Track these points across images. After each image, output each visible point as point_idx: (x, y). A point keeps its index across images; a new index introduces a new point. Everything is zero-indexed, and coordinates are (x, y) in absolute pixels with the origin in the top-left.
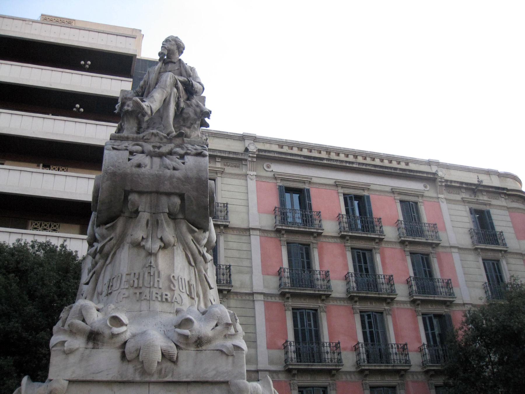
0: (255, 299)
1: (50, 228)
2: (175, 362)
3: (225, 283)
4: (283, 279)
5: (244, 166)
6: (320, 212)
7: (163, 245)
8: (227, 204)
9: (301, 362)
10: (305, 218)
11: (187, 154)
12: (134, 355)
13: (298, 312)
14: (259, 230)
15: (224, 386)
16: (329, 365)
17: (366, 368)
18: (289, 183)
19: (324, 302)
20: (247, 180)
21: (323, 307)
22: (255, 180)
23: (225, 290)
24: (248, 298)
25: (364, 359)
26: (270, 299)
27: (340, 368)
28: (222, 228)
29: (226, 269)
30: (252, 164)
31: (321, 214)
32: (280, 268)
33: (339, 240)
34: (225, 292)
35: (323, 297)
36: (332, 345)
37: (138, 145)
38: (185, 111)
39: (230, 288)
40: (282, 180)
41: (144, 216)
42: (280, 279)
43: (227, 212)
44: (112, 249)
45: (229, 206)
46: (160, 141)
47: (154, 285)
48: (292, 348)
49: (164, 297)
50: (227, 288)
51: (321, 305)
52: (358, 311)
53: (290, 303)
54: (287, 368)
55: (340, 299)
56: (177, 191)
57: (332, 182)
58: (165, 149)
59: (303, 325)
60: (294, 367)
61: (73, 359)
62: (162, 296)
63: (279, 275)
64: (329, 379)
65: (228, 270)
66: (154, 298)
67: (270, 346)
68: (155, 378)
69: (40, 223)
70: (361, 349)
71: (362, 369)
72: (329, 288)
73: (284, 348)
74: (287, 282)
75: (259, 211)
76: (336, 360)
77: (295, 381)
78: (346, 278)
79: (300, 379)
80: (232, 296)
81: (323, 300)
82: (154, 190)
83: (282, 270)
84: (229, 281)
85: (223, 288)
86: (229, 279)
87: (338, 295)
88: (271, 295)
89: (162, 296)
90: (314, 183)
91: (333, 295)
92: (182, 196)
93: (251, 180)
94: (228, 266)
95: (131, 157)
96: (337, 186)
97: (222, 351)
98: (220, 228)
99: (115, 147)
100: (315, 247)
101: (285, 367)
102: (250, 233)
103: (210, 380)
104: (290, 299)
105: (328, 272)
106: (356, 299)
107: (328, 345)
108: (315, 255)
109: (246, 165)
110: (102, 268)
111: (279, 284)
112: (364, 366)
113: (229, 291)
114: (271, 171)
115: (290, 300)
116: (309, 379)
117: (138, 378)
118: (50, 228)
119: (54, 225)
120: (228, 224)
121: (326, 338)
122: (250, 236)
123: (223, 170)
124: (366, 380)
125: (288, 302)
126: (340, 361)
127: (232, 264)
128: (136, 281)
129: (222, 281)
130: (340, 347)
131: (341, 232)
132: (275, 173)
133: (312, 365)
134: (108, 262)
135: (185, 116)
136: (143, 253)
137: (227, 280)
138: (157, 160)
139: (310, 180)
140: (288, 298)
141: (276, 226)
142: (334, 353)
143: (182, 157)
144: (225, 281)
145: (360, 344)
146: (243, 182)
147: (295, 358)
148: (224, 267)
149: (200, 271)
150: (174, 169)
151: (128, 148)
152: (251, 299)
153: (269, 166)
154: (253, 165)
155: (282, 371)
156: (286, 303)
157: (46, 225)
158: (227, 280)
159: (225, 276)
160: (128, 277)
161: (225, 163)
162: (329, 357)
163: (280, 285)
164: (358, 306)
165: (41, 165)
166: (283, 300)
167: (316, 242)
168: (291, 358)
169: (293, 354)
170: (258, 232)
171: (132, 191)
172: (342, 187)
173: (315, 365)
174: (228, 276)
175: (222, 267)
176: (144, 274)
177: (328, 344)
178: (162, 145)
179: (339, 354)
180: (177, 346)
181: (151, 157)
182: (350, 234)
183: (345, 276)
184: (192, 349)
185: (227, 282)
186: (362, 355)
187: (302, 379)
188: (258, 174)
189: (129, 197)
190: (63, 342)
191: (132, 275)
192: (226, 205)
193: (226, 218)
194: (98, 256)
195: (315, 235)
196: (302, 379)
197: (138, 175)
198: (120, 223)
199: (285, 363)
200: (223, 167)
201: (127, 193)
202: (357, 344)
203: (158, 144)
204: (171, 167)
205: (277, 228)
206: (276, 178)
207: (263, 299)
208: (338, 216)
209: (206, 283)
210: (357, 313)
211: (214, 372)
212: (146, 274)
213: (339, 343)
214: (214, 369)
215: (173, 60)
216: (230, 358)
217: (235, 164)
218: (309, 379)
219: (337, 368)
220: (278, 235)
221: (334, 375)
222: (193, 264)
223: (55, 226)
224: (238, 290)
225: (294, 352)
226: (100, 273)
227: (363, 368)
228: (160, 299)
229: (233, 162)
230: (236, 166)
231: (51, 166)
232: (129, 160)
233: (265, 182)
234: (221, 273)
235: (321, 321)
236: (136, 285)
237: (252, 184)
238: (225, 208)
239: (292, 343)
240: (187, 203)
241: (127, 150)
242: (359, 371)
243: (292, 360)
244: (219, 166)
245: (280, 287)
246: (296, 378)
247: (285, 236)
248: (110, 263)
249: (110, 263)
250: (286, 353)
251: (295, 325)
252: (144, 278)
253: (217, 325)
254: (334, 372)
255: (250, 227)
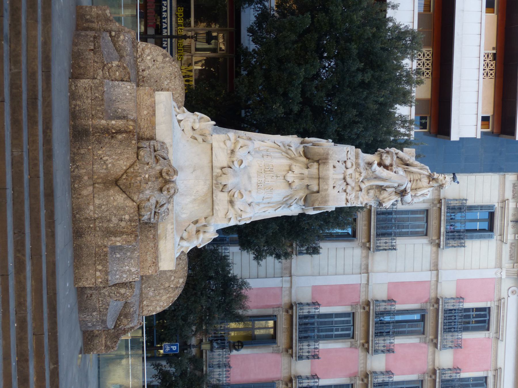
0: (362, 275)
1: (426, 69)
2: (222, 191)
3: (377, 244)
4: (384, 304)
5: (512, 265)
6: (461, 347)
7: (290, 182)
8: (464, 246)
9: (299, 318)
10: (453, 330)
11: (347, 193)
12: (225, 173)
13: (351, 319)
14: (437, 281)
15: (212, 213)
16: (296, 346)
17: (294, 384)
18: (495, 315)
19: (361, 346)
20: (495, 268)
21: (356, 345)
22: (494, 276)
23: (370, 245)
24: (363, 267)
25: (302, 383)
26: (363, 289)
27: (294, 357)
28: (437, 241)
29: (392, 246)
30: (514, 273)
31: (460, 349)
32: (395, 302)
33: (431, 367)
34: (368, 245)
35: (366, 346)
36: (316, 350)
37: (352, 165)
38: (385, 192)
39: (371, 249)
40: (498, 307)
41: (306, 172)
42: (383, 301)
43: (455, 247)
44: (290, 155)
45: (463, 248)
46: (357, 178)
47: (267, 179)
48: (313, 311)
49: (260, 185)
50: (372, 246)
51: (358, 342)
52: (353, 382)
53: (359, 310)
54: (293, 304)
55: (365, 363)
56: (320, 189)
57: (500, 364)
58: (349, 180)
59: (336, 322)
60: (294, 311)
61: (222, 145)
62: (260, 183)
63: (389, 300)
64: (284, 347)
65: (390, 248)
66: (259, 179)
67: (316, 289)
68: (214, 182)
69: (429, 59)
70: (313, 381)
71: (292, 380)
72: (376, 351)
73: (313, 303)
74: (381, 307)
75: (458, 281)
76: (302, 354)
77: (281, 312)
78: (388, 372)
79: (283, 318)
80: (364, 251)
81: (363, 345)
82: (320, 176)
83: (393, 303)
84: (379, 248)
85: (372, 243)
86: (381, 248)
87: (369, 362)
88: (367, 292)
89: (260, 183)
90: (497, 344)
91: (369, 356)
92: (318, 192)
93: (496, 273)
94: (395, 248)
95: (340, 162)
96: (496, 370)
97: (228, 212)
98: (438, 239)
99: (349, 153)
100: (421, 340)
101: (295, 303)
102: (433, 270)
103: (214, 207)
104: (363, 310)
105: (393, 352)
106: (365, 380)
107: (316, 346)
108: (413, 340)
109: (514, 268)
110: (281, 150)
111: (378, 299)
112: (295, 383)
113: (369, 248)
114: (508, 295)
115: (362, 310)
116: (283, 326)
117: (214, 174)
118: (426, 69)
119: (429, 72)
120: (441, 247)
121: (323, 346)
122: (430, 271)
123: (504, 242)
124: (282, 384)
125: (361, 309)
126: (300, 358)
127: (398, 251)
128: (268, 170)
129: (379, 242)
130: (315, 359)
131: (439, 369)
132: (506, 299)
133: (296, 329)
134: (283, 153)
135: (382, 192)
136: (284, 173)
137: (380, 246)
138: (342, 176)
139: (500, 339)
140: (364, 308)
141: (442, 298)
142: (309, 352)
143: (345, 191)
144: (379, 245)
145: (317, 380)
146: (493, 263)
147: (303, 312)
148: (394, 244)
149: (282, 204)
150: (334, 187)
151: (349, 160)
152: (362, 271)
153: (514, 292)
154: (513, 275)
155: (291, 300)
156: (359, 306)
157: (428, 64)
158: (380, 246)
159: (385, 245)
160: (271, 166)
161: (514, 245)
162: (304, 347)
163: (377, 301)
164: (358, 382)
165: (494, 52)
166: (362, 304)
167: (427, 341)
168: (303, 309)
169: (307, 310)
170: (434, 279)
171: (319, 165)
172: (495, 376)
173: (296, 332)
174: (385, 248)
175: (393, 241)
176: (273, 174)
177: (317, 346)
178: (353, 179)
179: (308, 358)
180: (230, 191)
181: (343, 173)
182: (437, 380)
183: (390, 371)
184: (229, 199)
185: (378, 246)
186: (307, 381)
187: (283, 320)
188: (503, 280)
189: (315, 163)
190: (230, 139)
191: (272, 168)
192: (463, 245)
193: (448, 245)
194: (288, 147)
195: (435, 341)
196: (283, 320)
197: (328, 167)
198: (304, 159)
199: (299, 304)
200: (509, 242)
201: (318, 161)
202: (318, 377)
203: (353, 177)
204: (335, 185)
205: (439, 299)
206: (500, 300)
207: (363, 282)
208: (458, 368)
209: (277, 208)
210: (351, 380)
211: (217, 209)
212: (272, 175)
213: (318, 358)
214: (219, 209)
215: (431, 182)
216: (224, 216)
217: (513, 255)
218: (283, 326)
219: (294, 355)
220: (433, 300)
221: (287, 351)
222: (284, 200)
223: (428, 74)
224: (370, 258)
225: (309, 312)
226: (279, 149)
227: (294, 381)
228: (259, 182)
229: (516, 252)
230: (511, 256)
231: (494, 62)
232: (339, 161)
233: (494, 289)
234: (387, 241)
235: (342, 342)
236: (266, 170)
237: (491, 274)
238: (459, 245)
239: (318, 310)
240: (314, 194)
241: (347, 159)
242: (291, 378)
243: (301, 309)
244: (509, 238)
245: (375, 300)
246: (284, 313)
247: (432, 308)
248: (282, 155)
249: (282, 155)
250: (308, 304)
251: (338, 315)
252: (269, 173)
253: (242, 211)
254: (290, 351)
255: (439, 271)
